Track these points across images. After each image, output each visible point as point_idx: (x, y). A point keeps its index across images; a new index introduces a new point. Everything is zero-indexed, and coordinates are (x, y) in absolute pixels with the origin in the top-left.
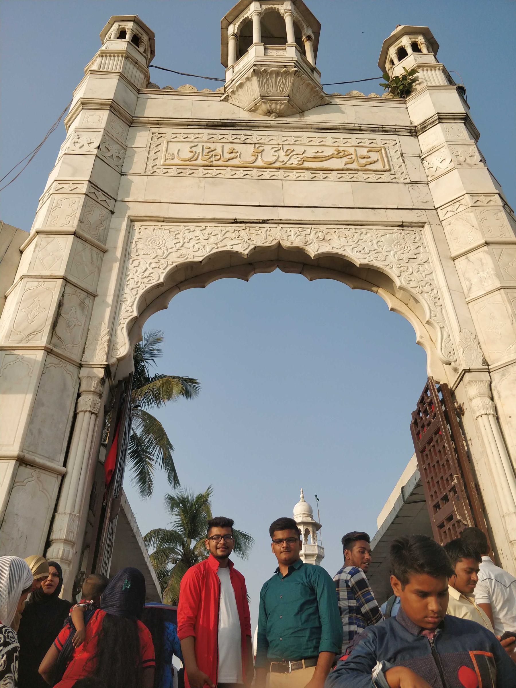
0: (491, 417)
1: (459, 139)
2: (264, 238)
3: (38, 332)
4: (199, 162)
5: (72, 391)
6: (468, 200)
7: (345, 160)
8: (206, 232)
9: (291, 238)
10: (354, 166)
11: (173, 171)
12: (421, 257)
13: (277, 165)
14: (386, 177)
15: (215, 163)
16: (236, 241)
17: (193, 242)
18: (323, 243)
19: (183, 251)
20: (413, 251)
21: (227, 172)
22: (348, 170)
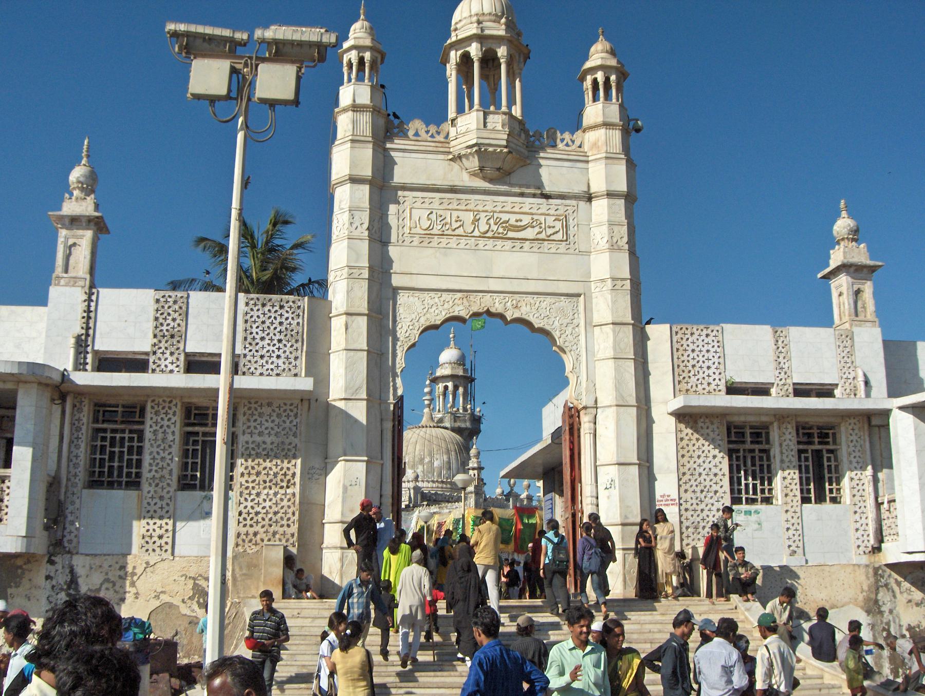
1: (617, 219)
3: (360, 388)
4: (434, 231)
5: (379, 420)
6: (609, 283)
7: (537, 230)
8: (442, 299)
10: (543, 236)
11: (416, 240)
13: (490, 234)
15: (446, 233)
16: (461, 307)
17: (434, 308)
19: (428, 316)
20: (571, 317)
21: (453, 242)
22: (537, 240)
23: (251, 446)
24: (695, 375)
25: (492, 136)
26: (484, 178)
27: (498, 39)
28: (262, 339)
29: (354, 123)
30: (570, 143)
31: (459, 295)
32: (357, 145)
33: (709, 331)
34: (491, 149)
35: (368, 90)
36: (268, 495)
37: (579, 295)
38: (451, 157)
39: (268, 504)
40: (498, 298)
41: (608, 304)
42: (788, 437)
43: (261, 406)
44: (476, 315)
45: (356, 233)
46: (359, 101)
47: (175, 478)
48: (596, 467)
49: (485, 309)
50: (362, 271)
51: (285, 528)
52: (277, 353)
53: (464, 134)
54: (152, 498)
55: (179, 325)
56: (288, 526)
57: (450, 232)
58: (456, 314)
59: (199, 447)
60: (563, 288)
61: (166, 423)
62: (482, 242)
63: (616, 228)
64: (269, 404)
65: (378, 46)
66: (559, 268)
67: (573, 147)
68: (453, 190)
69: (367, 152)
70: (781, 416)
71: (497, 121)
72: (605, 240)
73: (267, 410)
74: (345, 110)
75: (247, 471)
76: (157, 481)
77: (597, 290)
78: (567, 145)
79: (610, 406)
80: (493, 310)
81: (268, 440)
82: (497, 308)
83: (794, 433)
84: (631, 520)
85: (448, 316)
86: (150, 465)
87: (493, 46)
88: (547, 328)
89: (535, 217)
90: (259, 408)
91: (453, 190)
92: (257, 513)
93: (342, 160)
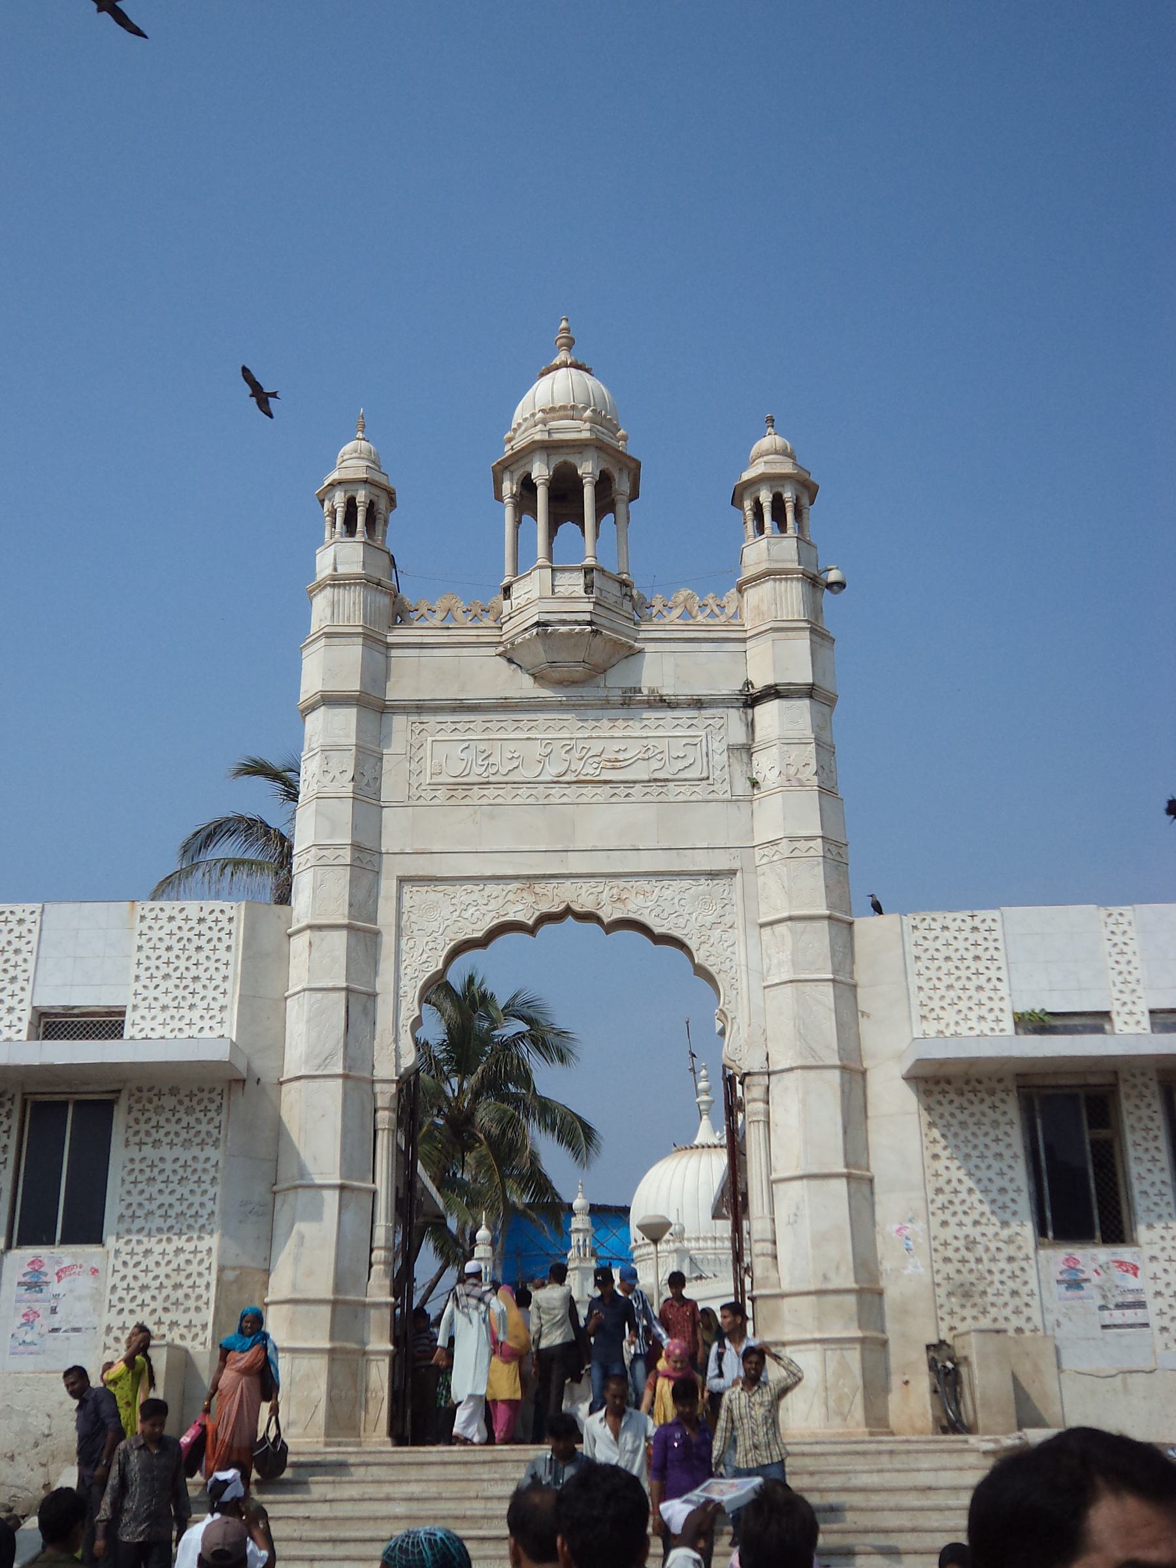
0: (761, 1124)
1: (796, 734)
2: (552, 898)
5: (370, 1109)
9: (583, 897)
11: (441, 793)
12: (728, 920)
14: (701, 791)
15: (491, 779)
17: (472, 910)
18: (618, 905)
20: (720, 912)
22: (656, 780)
23: (137, 1166)
24: (952, 1004)
26: (560, 683)
27: (578, 446)
29: (333, 604)
30: (717, 610)
31: (515, 885)
32: (336, 641)
33: (977, 922)
34: (563, 629)
35: (360, 548)
36: (163, 1253)
37: (732, 873)
38: (501, 649)
39: (162, 1271)
40: (586, 886)
41: (791, 885)
43: (160, 1095)
44: (546, 918)
45: (331, 789)
46: (342, 570)
48: (771, 1183)
49: (562, 906)
50: (341, 852)
51: (192, 1314)
52: (190, 1000)
53: (520, 610)
55: (25, 960)
56: (198, 1309)
58: (510, 917)
60: (704, 862)
62: (556, 791)
63: (795, 751)
64: (174, 1091)
65: (378, 477)
66: (706, 830)
67: (723, 619)
68: (505, 706)
69: (354, 652)
71: (573, 584)
72: (776, 771)
73: (169, 1102)
74: (321, 586)
75: (130, 1212)
77: (765, 860)
78: (712, 614)
79: (791, 1069)
80: (576, 908)
82: (585, 903)
84: (836, 1283)
85: (495, 922)
87: (573, 459)
88: (677, 933)
89: (651, 742)
90: (156, 1099)
91: (505, 706)
92: (144, 1288)
93: (324, 667)
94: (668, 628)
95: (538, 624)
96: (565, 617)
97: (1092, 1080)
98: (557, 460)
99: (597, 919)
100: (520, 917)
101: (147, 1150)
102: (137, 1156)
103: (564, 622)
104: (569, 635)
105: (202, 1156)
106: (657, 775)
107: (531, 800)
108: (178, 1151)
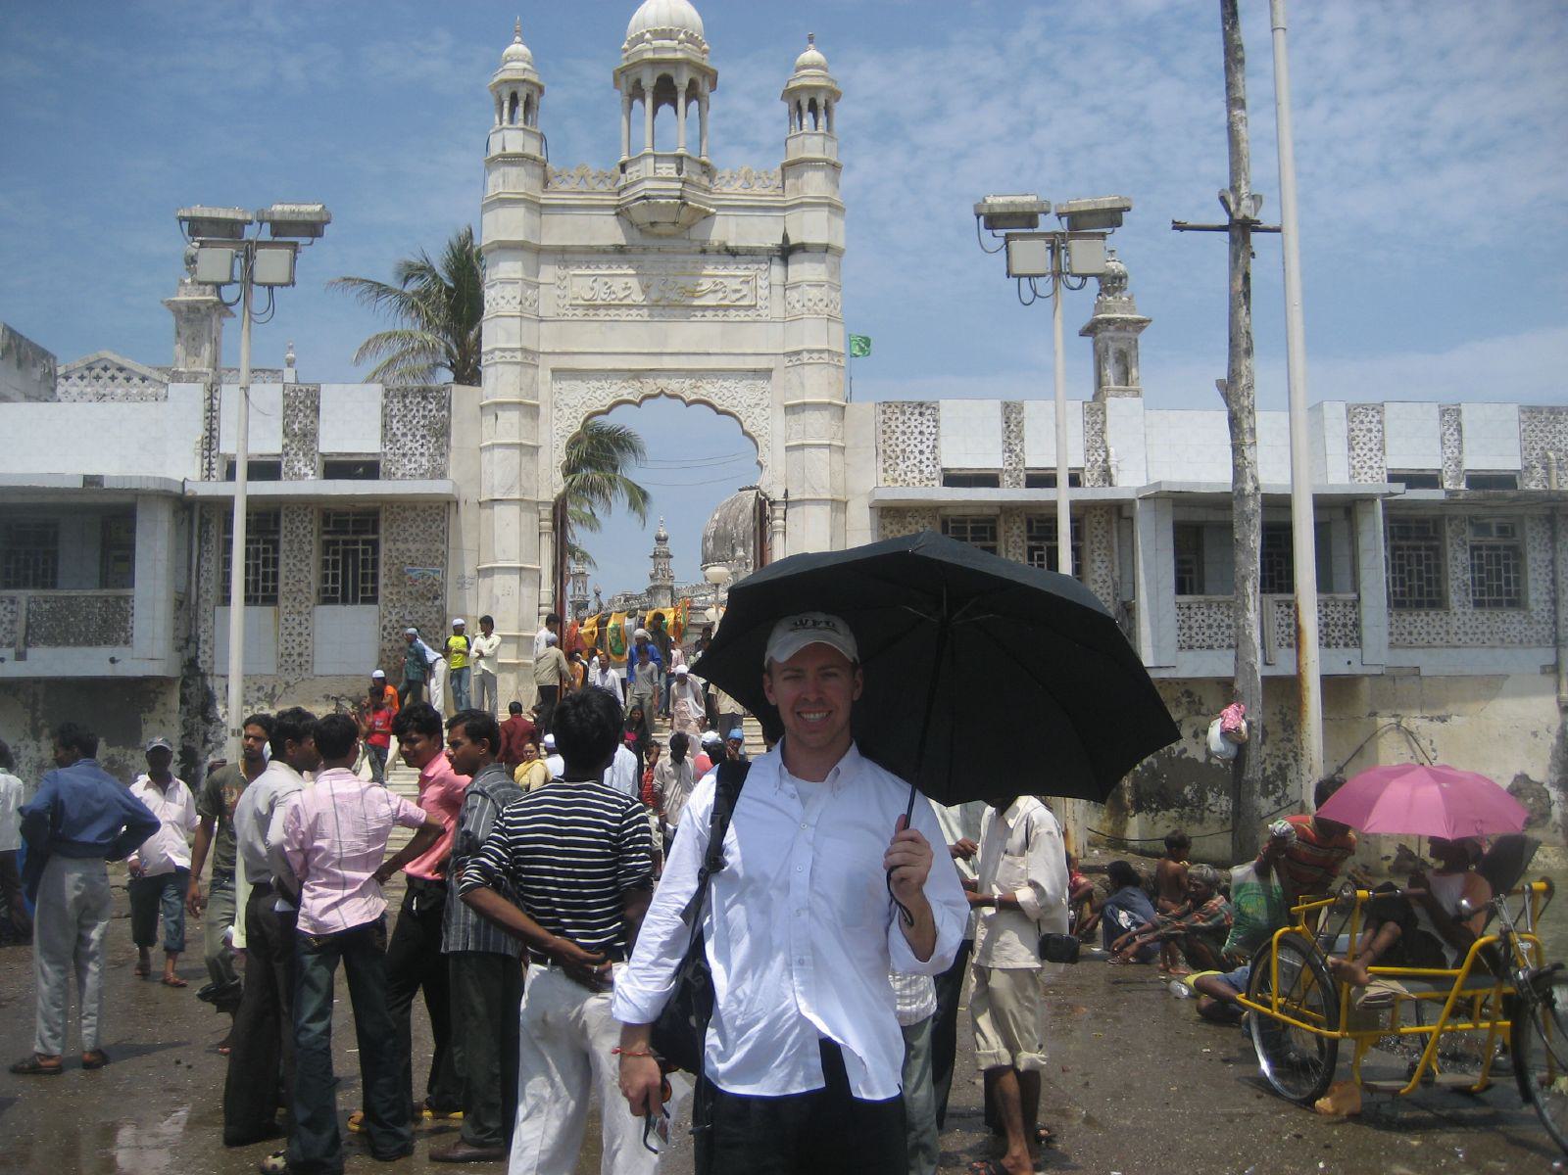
2: (651, 386)
7: (721, 295)
9: (674, 385)
18: (696, 390)
25: (664, 185)
27: (676, 63)
28: (404, 435)
42: (1016, 531)
47: (314, 591)
53: (634, 184)
54: (290, 613)
57: (617, 302)
59: (339, 557)
60: (751, 363)
61: (301, 531)
70: (1008, 509)
76: (295, 595)
81: (413, 547)
83: (1024, 528)
86: (287, 577)
87: (671, 72)
88: (731, 410)
89: (719, 280)
94: (734, 197)
95: (644, 197)
96: (662, 193)
97: (986, 511)
98: (659, 72)
99: (682, 399)
100: (631, 398)
101: (400, 545)
102: (393, 548)
103: (661, 197)
104: (667, 205)
105: (434, 548)
106: (726, 302)
107: (639, 318)
108: (418, 545)
